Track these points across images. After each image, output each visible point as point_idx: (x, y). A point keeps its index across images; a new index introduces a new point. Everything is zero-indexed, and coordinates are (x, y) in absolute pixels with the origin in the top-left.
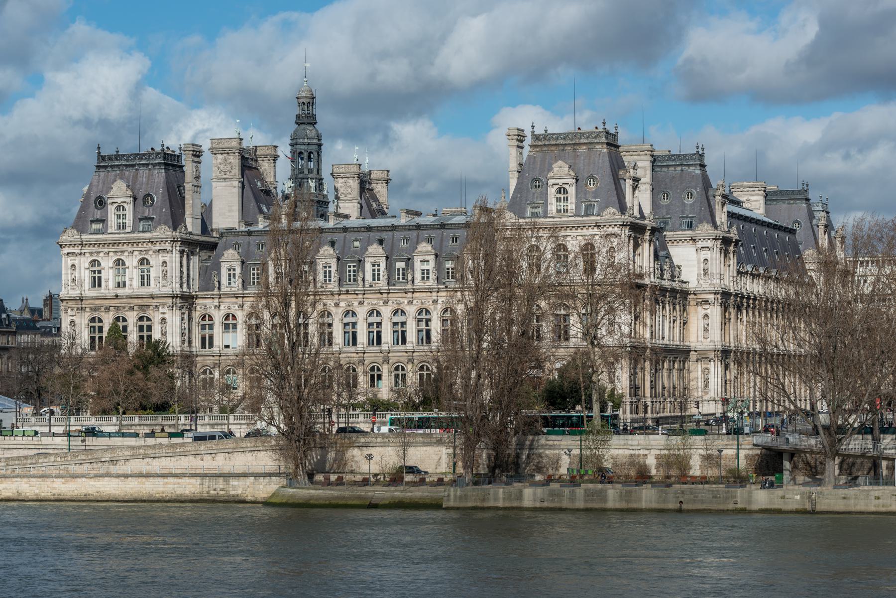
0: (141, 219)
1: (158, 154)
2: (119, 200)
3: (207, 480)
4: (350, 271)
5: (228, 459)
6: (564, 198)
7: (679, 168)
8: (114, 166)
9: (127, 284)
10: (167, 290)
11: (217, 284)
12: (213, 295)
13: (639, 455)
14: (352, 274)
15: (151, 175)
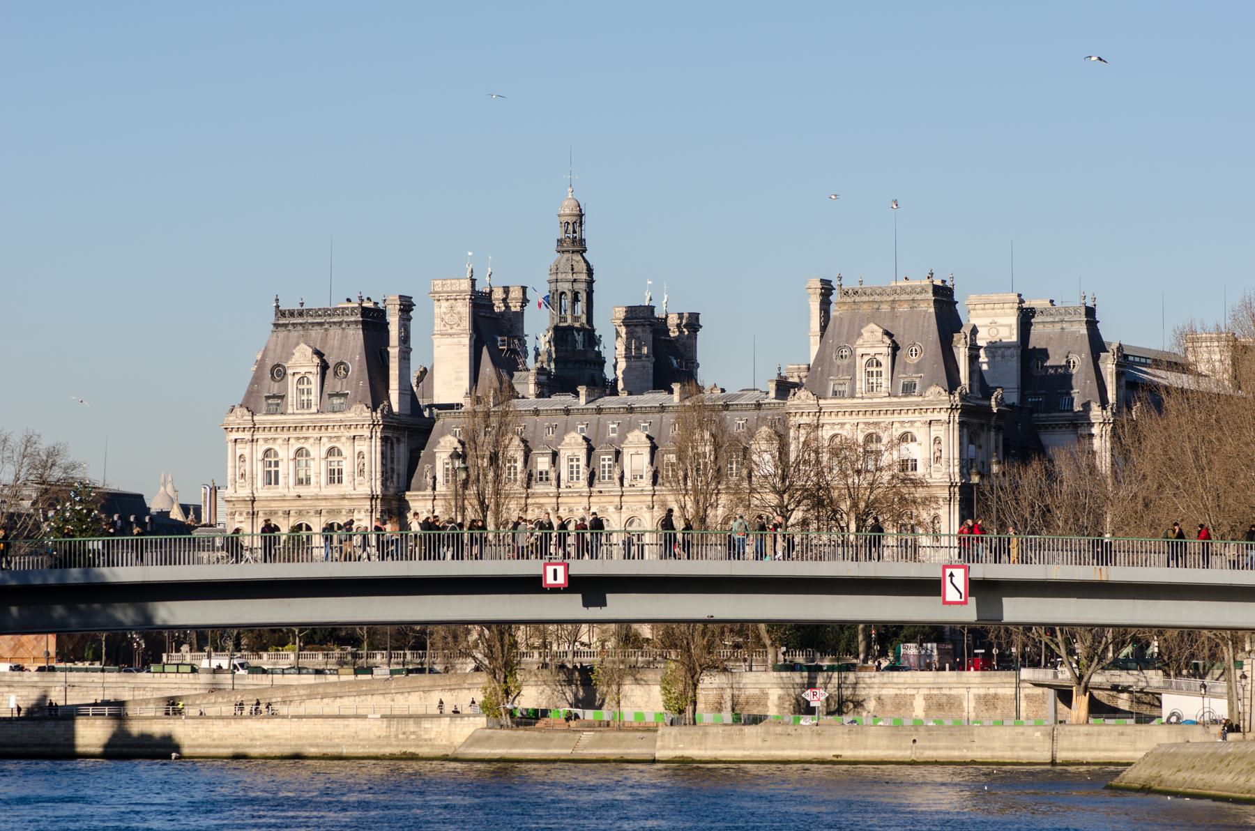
0: (331, 396)
1: (353, 309)
2: (303, 370)
3: (395, 722)
4: (604, 466)
5: (423, 699)
6: (877, 372)
7: (1058, 326)
8: (296, 324)
9: (313, 480)
10: (365, 490)
11: (429, 480)
12: (425, 496)
13: (905, 695)
14: (607, 469)
15: (344, 337)
